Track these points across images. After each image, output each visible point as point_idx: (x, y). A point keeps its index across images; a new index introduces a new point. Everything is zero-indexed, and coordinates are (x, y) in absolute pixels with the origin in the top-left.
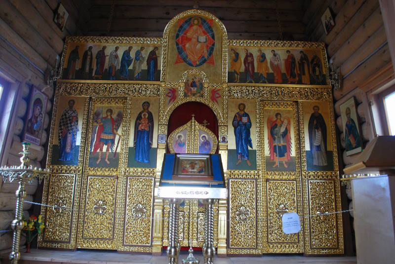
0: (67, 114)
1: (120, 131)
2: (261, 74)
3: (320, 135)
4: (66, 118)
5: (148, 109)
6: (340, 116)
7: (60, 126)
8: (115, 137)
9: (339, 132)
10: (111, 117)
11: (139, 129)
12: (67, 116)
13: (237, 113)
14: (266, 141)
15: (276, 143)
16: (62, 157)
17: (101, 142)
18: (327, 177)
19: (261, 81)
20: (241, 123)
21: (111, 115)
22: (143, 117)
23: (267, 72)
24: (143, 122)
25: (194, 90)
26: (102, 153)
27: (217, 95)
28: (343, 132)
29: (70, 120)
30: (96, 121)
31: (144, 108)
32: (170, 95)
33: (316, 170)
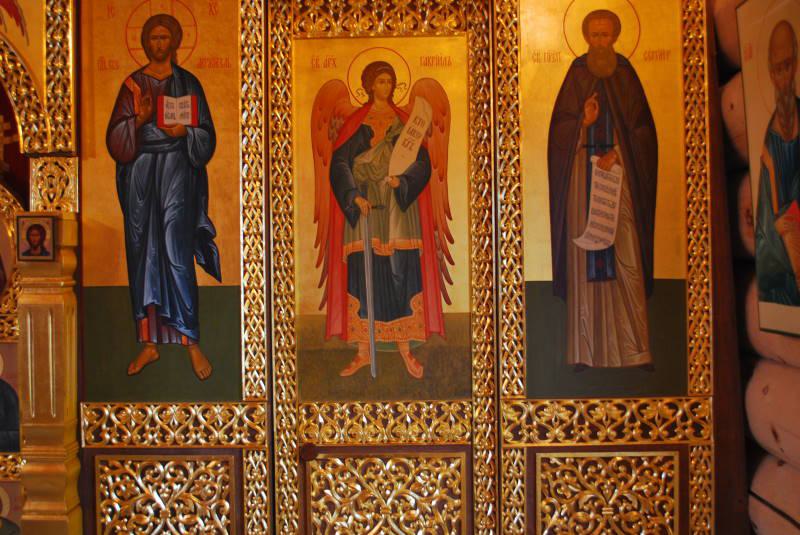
3: (618, 187)
9: (729, 164)
13: (133, 76)
15: (361, 240)
20: (155, 134)
33: (583, 394)
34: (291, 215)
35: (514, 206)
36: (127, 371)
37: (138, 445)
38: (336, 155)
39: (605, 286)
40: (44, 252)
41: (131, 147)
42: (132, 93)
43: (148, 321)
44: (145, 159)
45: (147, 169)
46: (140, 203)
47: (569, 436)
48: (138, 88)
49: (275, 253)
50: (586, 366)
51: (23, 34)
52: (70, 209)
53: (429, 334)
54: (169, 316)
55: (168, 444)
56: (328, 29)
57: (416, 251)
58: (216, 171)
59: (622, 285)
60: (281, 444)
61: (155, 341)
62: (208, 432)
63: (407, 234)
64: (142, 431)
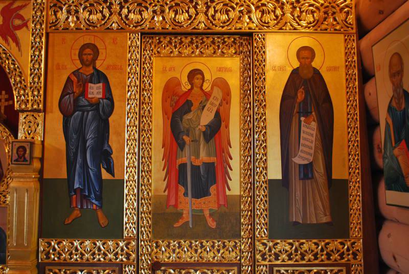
3: (314, 133)
6: (374, 76)
9: (369, 122)
13: (73, 73)
18: (329, 255)
20: (83, 102)
27: (18, 22)
28: (378, 124)
33: (296, 237)
34: (151, 144)
35: (263, 141)
36: (64, 222)
37: (68, 261)
39: (308, 182)
40: (25, 160)
41: (71, 108)
42: (72, 82)
43: (76, 196)
44: (78, 115)
45: (79, 120)
46: (75, 136)
47: (290, 259)
48: (76, 79)
49: (142, 163)
50: (299, 223)
51: (19, 51)
52: (39, 139)
53: (219, 205)
54: (87, 194)
55: (84, 261)
56: (171, 52)
57: (214, 163)
58: (113, 121)
59: (316, 181)
60: (142, 261)
61: (79, 207)
62: (105, 254)
63: (209, 155)
64: (71, 254)
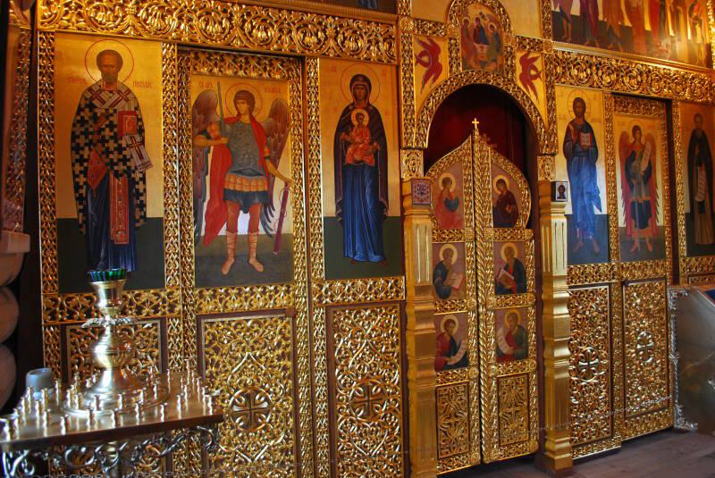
0: (96, 102)
1: (286, 166)
2: (611, 29)
4: (95, 118)
5: (366, 97)
7: (76, 149)
8: (271, 186)
10: (252, 118)
11: (348, 160)
12: (99, 112)
13: (571, 122)
14: (620, 192)
16: (101, 263)
17: (228, 202)
19: (611, 46)
21: (251, 110)
22: (355, 123)
23: (620, 23)
24: (357, 140)
25: (482, 49)
26: (236, 237)
27: (533, 72)
29: (111, 126)
30: (204, 132)
31: (355, 96)
32: (425, 59)
38: (627, 161)
63: (647, 195)
